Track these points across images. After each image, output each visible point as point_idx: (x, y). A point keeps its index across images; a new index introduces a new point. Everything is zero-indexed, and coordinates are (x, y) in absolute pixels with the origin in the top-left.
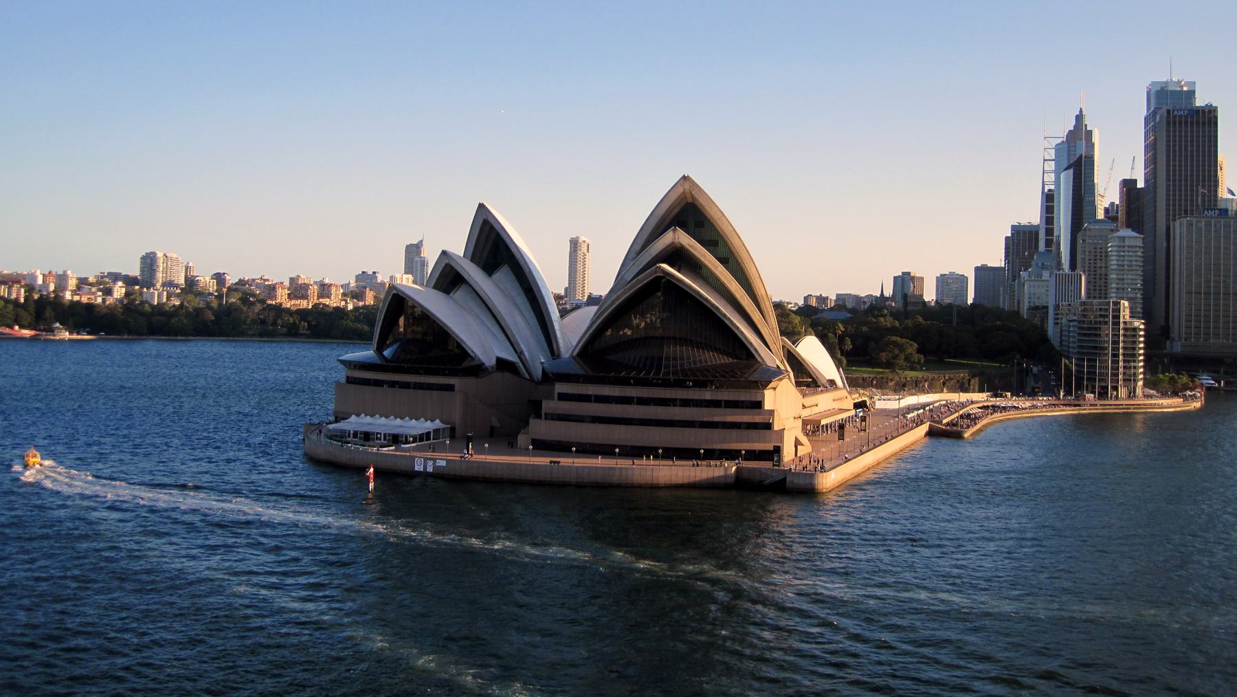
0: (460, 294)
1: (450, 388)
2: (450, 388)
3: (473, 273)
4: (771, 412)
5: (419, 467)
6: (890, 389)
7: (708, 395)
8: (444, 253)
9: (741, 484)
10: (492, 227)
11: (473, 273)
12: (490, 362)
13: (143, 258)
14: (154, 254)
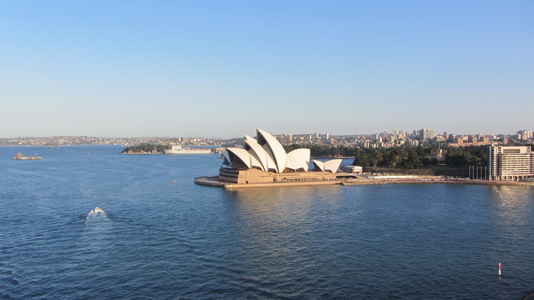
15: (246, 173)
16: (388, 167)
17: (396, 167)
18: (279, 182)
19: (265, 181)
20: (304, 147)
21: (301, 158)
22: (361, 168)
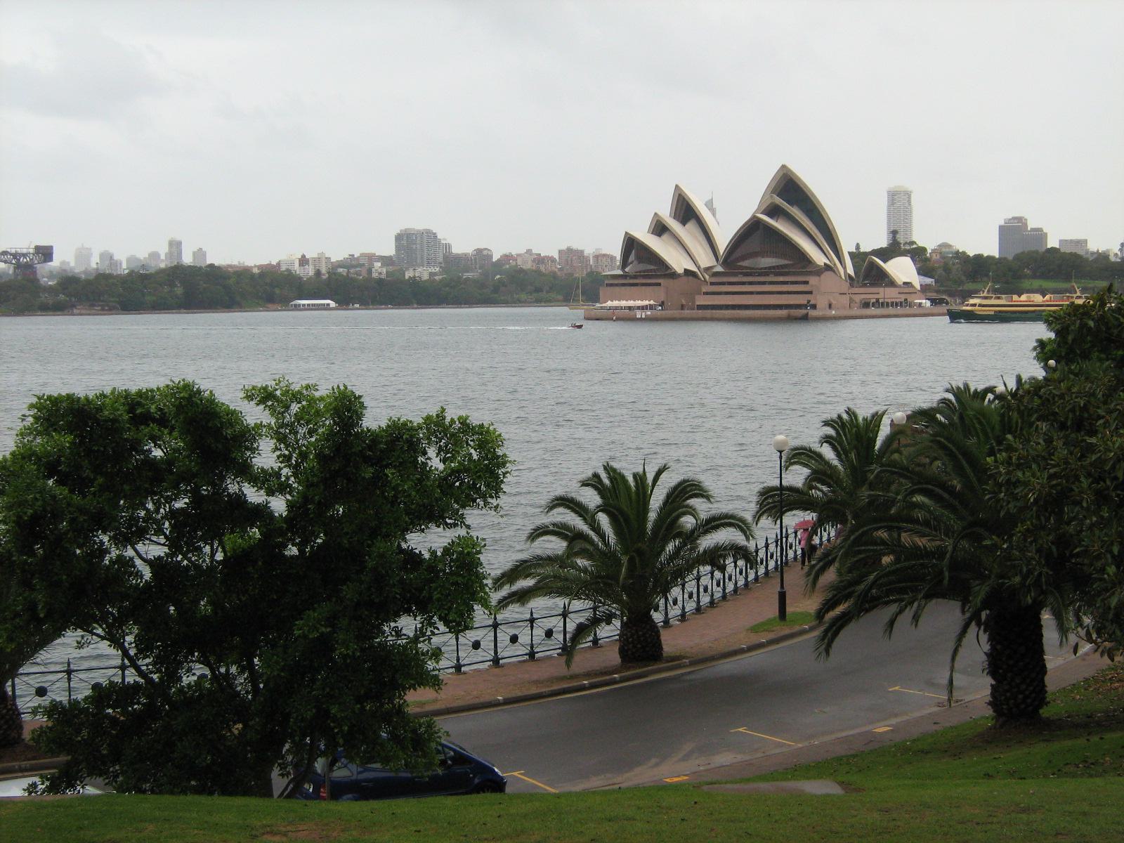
0: (665, 236)
1: (659, 284)
2: (659, 284)
3: (674, 225)
4: (812, 286)
7: (781, 279)
8: (656, 214)
10: (684, 198)
11: (674, 225)
12: (680, 271)
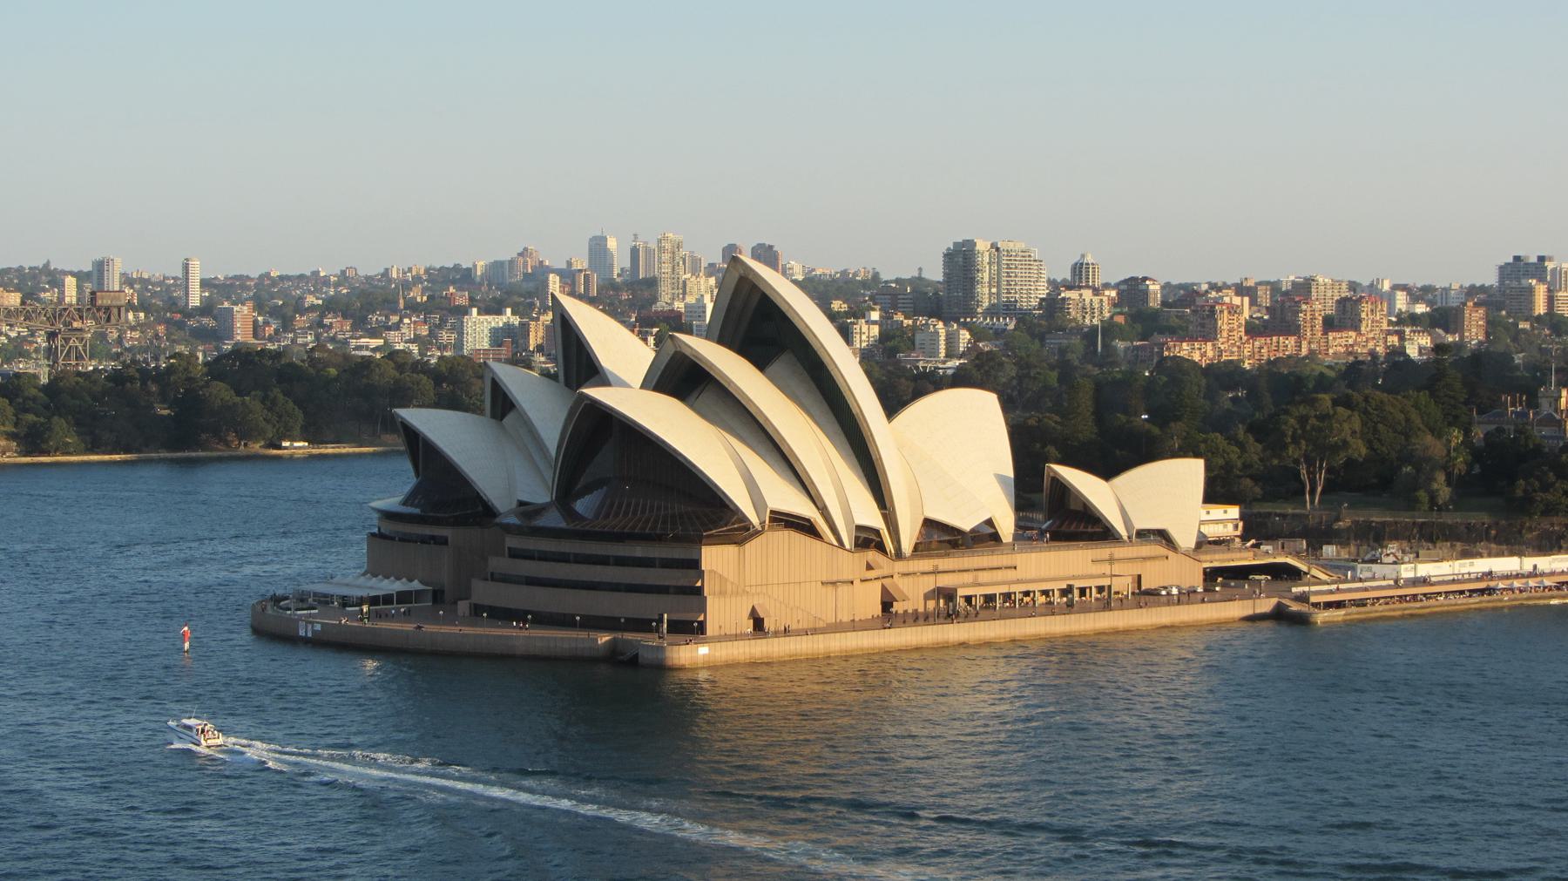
1: (443, 541)
5: (302, 633)
6: (1528, 544)
7: (639, 551)
9: (614, 656)
13: (949, 257)
14: (970, 244)
15: (741, 561)
16: (1411, 504)
17: (1458, 502)
18: (917, 618)
19: (845, 617)
20: (960, 380)
21: (955, 454)
22: (1234, 512)
